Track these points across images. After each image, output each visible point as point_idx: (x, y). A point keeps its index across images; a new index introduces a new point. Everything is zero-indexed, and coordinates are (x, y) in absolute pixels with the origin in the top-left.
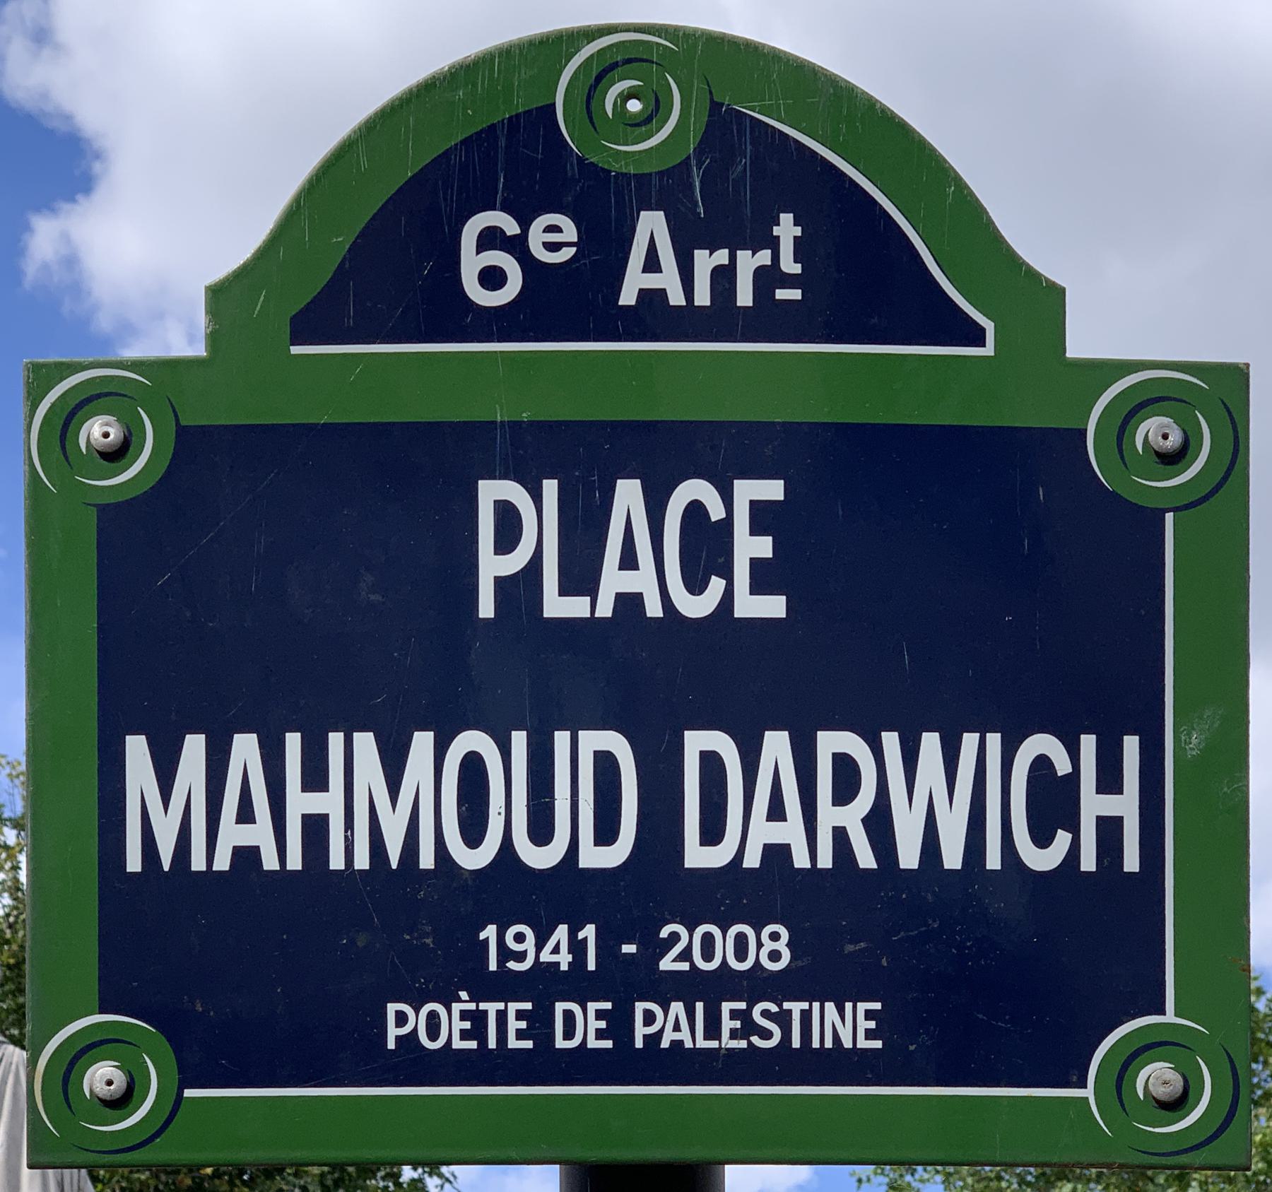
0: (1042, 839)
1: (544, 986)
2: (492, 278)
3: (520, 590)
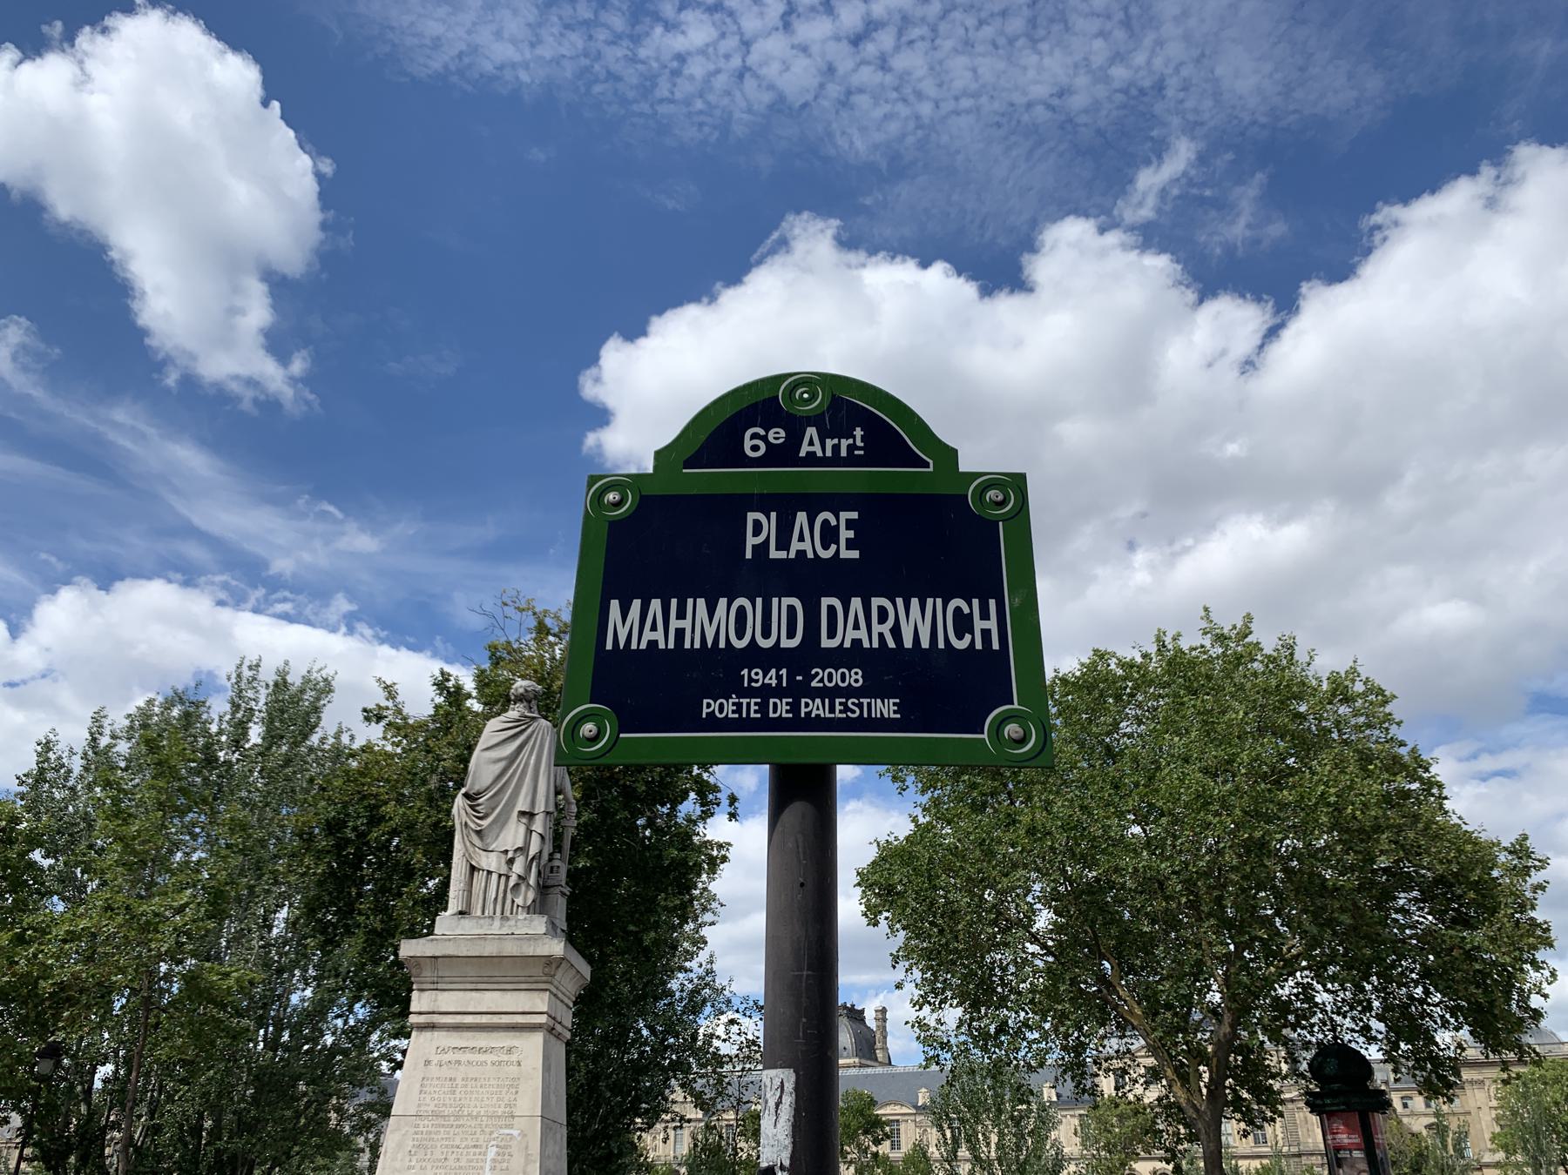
0: (960, 637)
1: (765, 692)
2: (755, 448)
3: (762, 549)
